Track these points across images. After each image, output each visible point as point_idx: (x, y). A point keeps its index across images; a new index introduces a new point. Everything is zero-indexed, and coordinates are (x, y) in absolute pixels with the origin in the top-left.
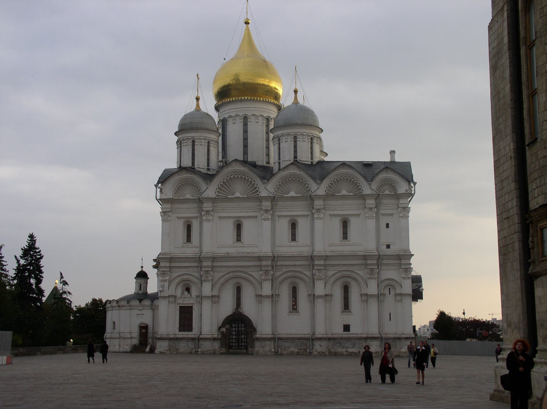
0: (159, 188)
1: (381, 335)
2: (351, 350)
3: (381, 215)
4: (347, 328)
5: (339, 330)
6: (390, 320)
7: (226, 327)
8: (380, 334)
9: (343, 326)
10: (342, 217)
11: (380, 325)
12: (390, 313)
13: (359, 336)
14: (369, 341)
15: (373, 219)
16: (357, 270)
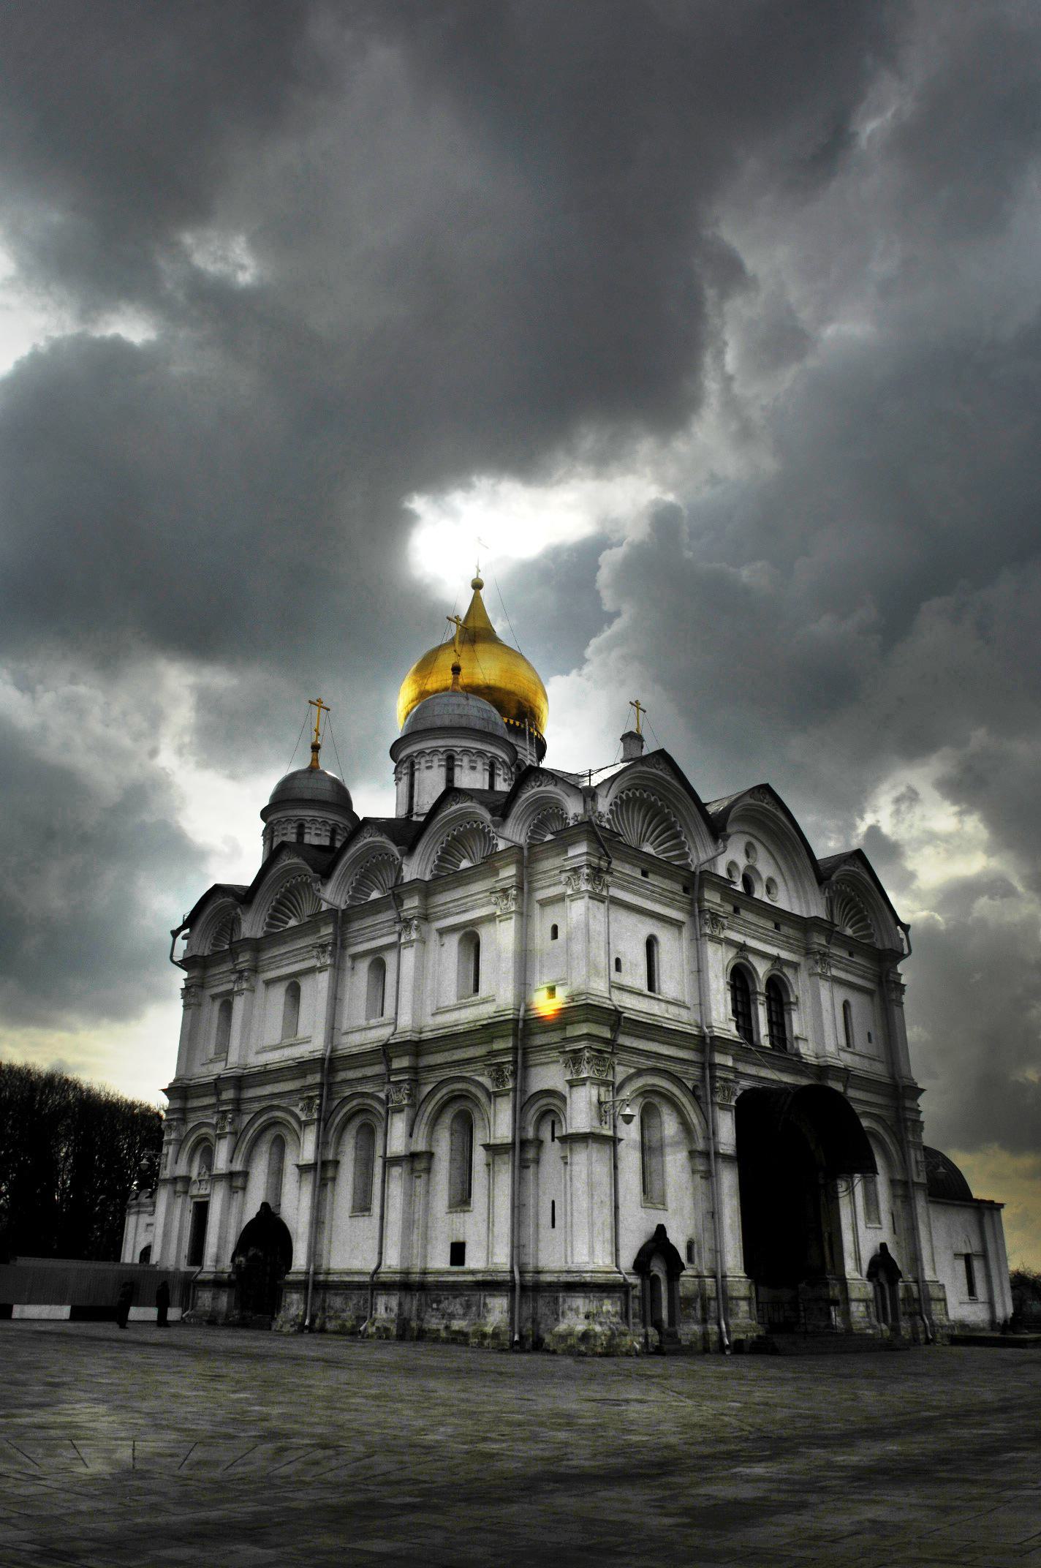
0: (184, 938)
1: (513, 1277)
2: (457, 1325)
3: (537, 906)
4: (458, 1252)
5: (440, 1260)
6: (553, 1226)
7: (251, 1253)
8: (512, 1272)
9: (448, 1250)
10: (462, 932)
11: (517, 1247)
12: (553, 1202)
13: (479, 1277)
14: (485, 1296)
15: (511, 918)
16: (479, 1075)
